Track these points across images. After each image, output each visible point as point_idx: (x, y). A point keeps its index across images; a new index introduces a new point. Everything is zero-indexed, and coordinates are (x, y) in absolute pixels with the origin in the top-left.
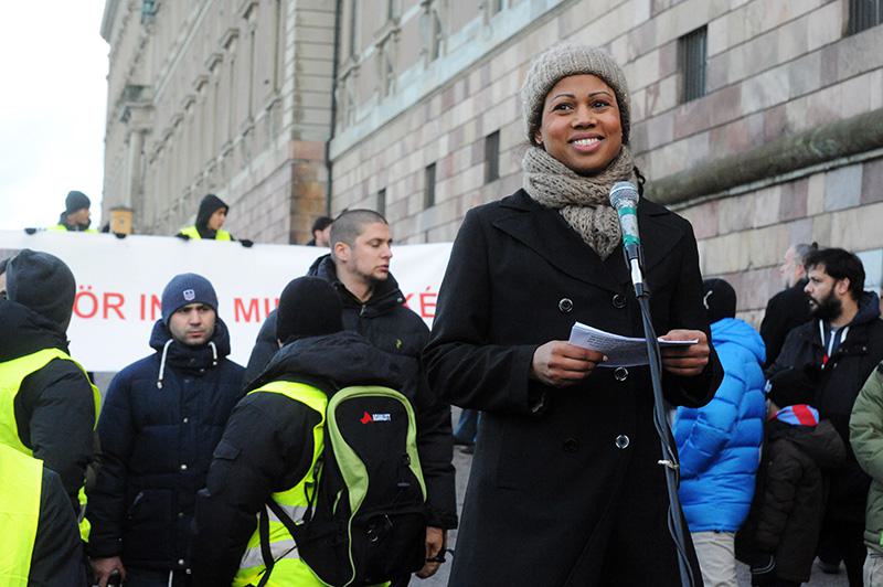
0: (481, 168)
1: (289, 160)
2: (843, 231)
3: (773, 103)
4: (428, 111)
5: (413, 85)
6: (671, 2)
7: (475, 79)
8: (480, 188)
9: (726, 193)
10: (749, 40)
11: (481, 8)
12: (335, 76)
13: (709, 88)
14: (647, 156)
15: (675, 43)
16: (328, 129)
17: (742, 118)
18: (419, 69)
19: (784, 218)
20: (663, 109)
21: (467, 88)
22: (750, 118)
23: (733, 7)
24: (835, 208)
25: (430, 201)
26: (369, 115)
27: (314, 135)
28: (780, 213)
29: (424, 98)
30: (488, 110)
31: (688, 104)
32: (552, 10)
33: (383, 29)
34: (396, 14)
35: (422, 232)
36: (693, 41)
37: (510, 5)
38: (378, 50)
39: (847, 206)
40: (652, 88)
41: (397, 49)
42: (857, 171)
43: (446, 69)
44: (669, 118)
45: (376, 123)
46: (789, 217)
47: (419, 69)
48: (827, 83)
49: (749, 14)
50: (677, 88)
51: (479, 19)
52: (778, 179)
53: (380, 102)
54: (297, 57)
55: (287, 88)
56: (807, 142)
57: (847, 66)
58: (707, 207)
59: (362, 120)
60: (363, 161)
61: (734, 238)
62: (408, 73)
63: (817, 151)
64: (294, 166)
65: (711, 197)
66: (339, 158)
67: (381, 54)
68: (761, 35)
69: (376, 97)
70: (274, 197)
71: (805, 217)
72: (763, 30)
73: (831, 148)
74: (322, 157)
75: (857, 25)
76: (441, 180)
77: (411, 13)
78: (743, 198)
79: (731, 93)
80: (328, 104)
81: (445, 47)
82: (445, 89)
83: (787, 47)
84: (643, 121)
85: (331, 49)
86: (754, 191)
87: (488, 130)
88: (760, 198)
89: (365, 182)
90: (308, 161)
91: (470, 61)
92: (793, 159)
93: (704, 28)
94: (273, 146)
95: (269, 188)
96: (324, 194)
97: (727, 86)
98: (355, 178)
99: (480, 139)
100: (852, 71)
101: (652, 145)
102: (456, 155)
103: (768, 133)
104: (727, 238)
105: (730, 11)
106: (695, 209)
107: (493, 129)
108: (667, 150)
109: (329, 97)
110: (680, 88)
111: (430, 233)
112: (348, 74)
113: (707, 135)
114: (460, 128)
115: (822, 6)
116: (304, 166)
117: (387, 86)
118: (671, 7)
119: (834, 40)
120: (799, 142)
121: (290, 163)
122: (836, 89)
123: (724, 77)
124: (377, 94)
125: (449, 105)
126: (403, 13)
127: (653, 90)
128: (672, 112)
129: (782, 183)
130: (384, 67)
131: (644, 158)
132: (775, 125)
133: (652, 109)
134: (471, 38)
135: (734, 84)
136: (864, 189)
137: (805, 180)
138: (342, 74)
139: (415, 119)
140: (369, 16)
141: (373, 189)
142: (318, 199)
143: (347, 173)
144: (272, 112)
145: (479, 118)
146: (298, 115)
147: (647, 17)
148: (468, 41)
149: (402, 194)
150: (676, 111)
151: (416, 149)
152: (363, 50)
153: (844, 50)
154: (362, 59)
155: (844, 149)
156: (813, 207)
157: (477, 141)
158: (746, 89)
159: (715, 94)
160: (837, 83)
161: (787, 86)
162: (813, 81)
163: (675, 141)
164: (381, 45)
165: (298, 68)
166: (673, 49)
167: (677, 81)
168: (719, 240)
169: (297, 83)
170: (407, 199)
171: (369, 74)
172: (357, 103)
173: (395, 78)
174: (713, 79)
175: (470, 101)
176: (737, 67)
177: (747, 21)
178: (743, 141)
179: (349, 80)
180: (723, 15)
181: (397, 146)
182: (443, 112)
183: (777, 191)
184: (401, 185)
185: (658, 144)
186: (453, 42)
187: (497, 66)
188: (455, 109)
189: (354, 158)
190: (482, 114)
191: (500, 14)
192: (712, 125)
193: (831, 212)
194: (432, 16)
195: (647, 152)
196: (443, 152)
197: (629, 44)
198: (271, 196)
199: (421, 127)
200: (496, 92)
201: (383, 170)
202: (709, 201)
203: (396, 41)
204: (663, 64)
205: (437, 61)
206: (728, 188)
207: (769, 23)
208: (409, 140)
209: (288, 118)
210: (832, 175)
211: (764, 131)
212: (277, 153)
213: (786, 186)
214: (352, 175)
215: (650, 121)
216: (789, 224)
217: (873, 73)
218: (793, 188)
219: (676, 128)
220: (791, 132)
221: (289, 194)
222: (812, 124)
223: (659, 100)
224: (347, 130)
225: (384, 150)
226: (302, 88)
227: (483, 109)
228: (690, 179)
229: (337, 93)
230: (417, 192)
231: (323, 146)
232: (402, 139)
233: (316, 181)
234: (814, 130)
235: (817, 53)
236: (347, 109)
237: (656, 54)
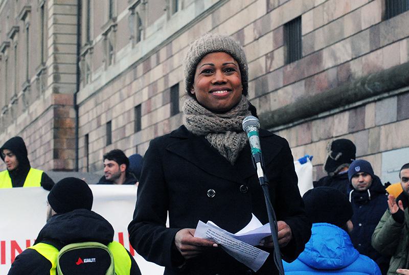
0: (168, 107)
1: (52, 105)
2: (387, 137)
3: (342, 62)
4: (135, 74)
5: (126, 57)
6: (279, 2)
7: (163, 53)
8: (168, 119)
9: (316, 117)
10: (327, 24)
11: (165, 10)
12: (78, 53)
13: (303, 54)
14: (267, 96)
15: (282, 28)
16: (75, 86)
17: (324, 71)
18: (129, 48)
19: (351, 130)
20: (276, 68)
21: (158, 58)
22: (329, 71)
23: (316, 5)
24: (381, 123)
25: (138, 128)
26: (100, 76)
27: (67, 90)
28: (349, 127)
29: (132, 65)
30: (172, 71)
31: (291, 64)
32: (208, 10)
33: (107, 24)
34: (114, 15)
35: (133, 147)
36: (292, 27)
37: (182, 8)
38: (104, 37)
39: (389, 122)
40: (269, 55)
41: (115, 36)
42: (394, 101)
43: (145, 47)
44: (280, 74)
45: (104, 82)
46: (354, 130)
47: (129, 48)
48: (374, 48)
49: (325, 8)
51: (164, 17)
52: (347, 107)
53: (106, 69)
54: (55, 43)
55: (50, 62)
56: (363, 84)
57: (385, 38)
58: (305, 126)
59: (96, 80)
60: (97, 105)
62: (122, 50)
63: (369, 89)
64: (55, 109)
65: (307, 119)
66: (83, 103)
67: (106, 39)
68: (334, 21)
69: (103, 67)
70: (43, 128)
71: (365, 130)
72: (334, 19)
73: (378, 87)
74: (72, 103)
75: (390, 14)
76: (145, 115)
77: (123, 15)
78: (327, 120)
79: (317, 56)
80: (75, 71)
81: (144, 34)
82: (145, 59)
83: (349, 28)
84: (263, 75)
85: (75, 37)
87: (171, 84)
89: (99, 117)
90: (63, 106)
91: (159, 43)
92: (356, 94)
93: (299, 19)
94: (42, 97)
95: (40, 123)
96: (74, 125)
97: (315, 52)
98: (93, 115)
99: (168, 89)
100: (389, 40)
101: (270, 89)
102: (153, 98)
103: (339, 78)
104: (317, 143)
105: (314, 8)
106: (297, 127)
107: (175, 83)
108: (280, 92)
109: (75, 67)
110: (286, 55)
111: (138, 147)
112: (86, 52)
113: (303, 82)
114: (155, 84)
115: (369, 2)
116: (61, 109)
117: (110, 59)
118: (279, 6)
119: (377, 22)
120: (359, 85)
121: (52, 107)
122: (379, 52)
123: (313, 47)
124: (104, 64)
125: (147, 70)
126: (118, 14)
127: (270, 56)
128: (281, 69)
129: (349, 110)
130: (108, 48)
131: (266, 97)
132: (343, 75)
133: (270, 68)
134: (160, 28)
135: (317, 51)
136: (399, 110)
137: (363, 107)
138: (82, 52)
139: (128, 78)
140: (98, 17)
141: (104, 121)
142: (70, 128)
143: (88, 112)
144: (41, 76)
145: (166, 77)
146: (56, 78)
147: (265, 13)
148: (158, 30)
149: (121, 124)
151: (129, 97)
152: (95, 37)
153: (383, 28)
154: (94, 43)
155: (386, 88)
156: (369, 123)
157: (165, 90)
158: (325, 54)
160: (380, 48)
161: (350, 51)
162: (365, 47)
163: (284, 86)
164: (106, 34)
165: (56, 49)
166: (281, 31)
167: (284, 50)
168: (313, 144)
169: (55, 59)
170: (124, 127)
172: (92, 70)
173: (115, 54)
174: (305, 51)
175: (160, 66)
177: (325, 13)
178: (325, 85)
179: (87, 56)
180: (311, 9)
181: (117, 95)
182: (144, 74)
183: (347, 114)
184: (121, 118)
185: (274, 89)
186: (149, 31)
187: (176, 45)
188: (151, 71)
189: (91, 103)
190: (168, 74)
191: (176, 14)
192: (306, 76)
193: (379, 126)
194: (136, 15)
195: (268, 93)
196: (145, 98)
197: (254, 29)
198: (41, 127)
199: (131, 83)
200: (176, 60)
201: (109, 109)
202: (306, 122)
203: (115, 31)
205: (140, 43)
206: (317, 114)
207: (338, 14)
208: (124, 91)
209: (50, 80)
210: (379, 103)
211: (338, 79)
212: (45, 101)
213: (351, 111)
214: (90, 113)
215: (269, 75)
216: (354, 134)
217: (401, 42)
218: (356, 112)
219: (284, 79)
220: (354, 79)
221: (53, 126)
222: (366, 73)
223: (274, 62)
224: (87, 86)
225: (109, 98)
226: (59, 61)
227: (168, 72)
228: (294, 109)
229: (80, 63)
230: (130, 122)
231: (73, 96)
232: (120, 90)
233: (68, 117)
235: (368, 30)
236: (86, 73)
237: (271, 34)
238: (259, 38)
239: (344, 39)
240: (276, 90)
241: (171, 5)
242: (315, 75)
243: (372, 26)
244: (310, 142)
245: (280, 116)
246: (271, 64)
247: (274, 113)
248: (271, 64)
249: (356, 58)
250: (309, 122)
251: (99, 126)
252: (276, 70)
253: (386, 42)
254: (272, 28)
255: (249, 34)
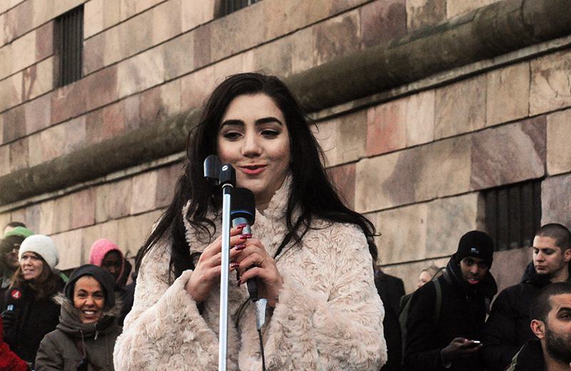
3: (148, 86)
9: (103, 179)
10: (125, 21)
13: (85, 71)
14: (24, 141)
15: (51, 24)
17: (118, 101)
20: (41, 93)
22: (126, 100)
31: (65, 87)
36: (68, 25)
50: (54, 70)
52: (153, 164)
56: (180, 125)
57: (220, 48)
58: (85, 194)
61: (112, 225)
65: (87, 183)
72: (138, 12)
78: (121, 184)
79: (107, 75)
83: (161, 30)
86: (131, 176)
88: (138, 183)
92: (167, 143)
93: (80, 9)
97: (104, 68)
103: (143, 116)
106: (72, 197)
108: (45, 135)
113: (84, 119)
119: (207, 20)
120: (173, 126)
123: (100, 60)
127: (30, 73)
132: (151, 107)
133: (30, 93)
150: (53, 93)
153: (216, 30)
158: (122, 71)
159: (91, 76)
161: (162, 69)
162: (186, 61)
163: (53, 126)
166: (50, 27)
168: (97, 227)
174: (89, 64)
176: (113, 48)
192: (89, 108)
197: (5, 25)
202: (86, 188)
204: (40, 45)
206: (105, 175)
211: (140, 115)
213: (162, 171)
215: (26, 105)
220: (166, 115)
222: (186, 107)
228: (67, 166)
234: (187, 113)
238: (14, 40)
239: (153, 47)
240: (39, 132)
242: (103, 107)
243: (199, 26)
244: (93, 223)
245: (42, 177)
246: (31, 87)
247: (32, 171)
248: (31, 87)
249: (170, 81)
250: (92, 189)
252: (40, 96)
253: (222, 56)
254: (35, 26)
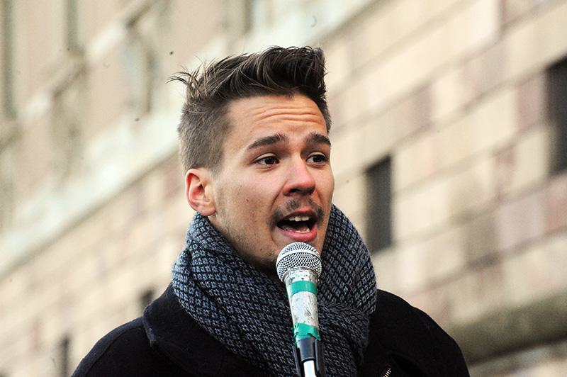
45: (53, 221)
60: (34, 287)
77: (105, 40)
89: (36, 327)
127: (505, 155)
139: (119, 216)
141: (51, 335)
171: (39, 143)
204: (522, 109)
208: (111, 252)
241: (236, 12)
251: (37, 347)
255: (448, 96)
